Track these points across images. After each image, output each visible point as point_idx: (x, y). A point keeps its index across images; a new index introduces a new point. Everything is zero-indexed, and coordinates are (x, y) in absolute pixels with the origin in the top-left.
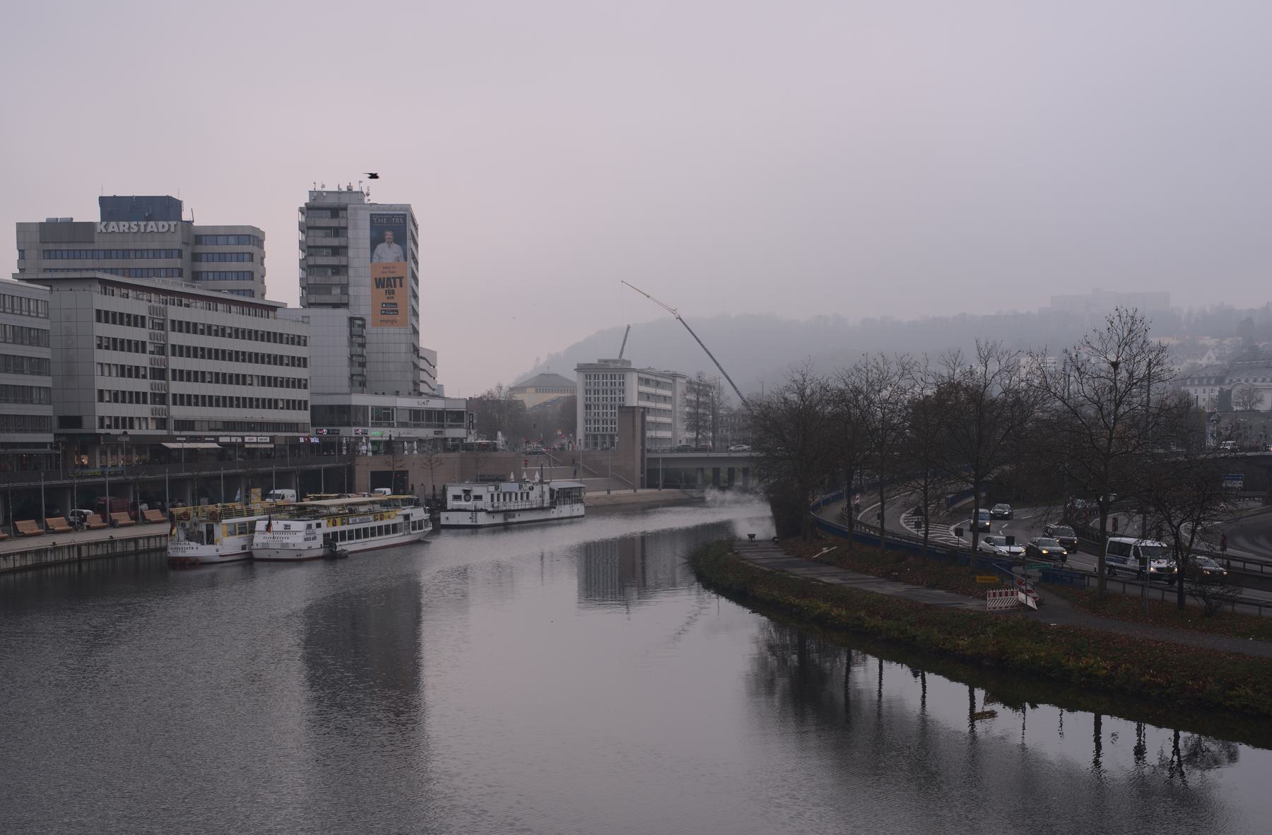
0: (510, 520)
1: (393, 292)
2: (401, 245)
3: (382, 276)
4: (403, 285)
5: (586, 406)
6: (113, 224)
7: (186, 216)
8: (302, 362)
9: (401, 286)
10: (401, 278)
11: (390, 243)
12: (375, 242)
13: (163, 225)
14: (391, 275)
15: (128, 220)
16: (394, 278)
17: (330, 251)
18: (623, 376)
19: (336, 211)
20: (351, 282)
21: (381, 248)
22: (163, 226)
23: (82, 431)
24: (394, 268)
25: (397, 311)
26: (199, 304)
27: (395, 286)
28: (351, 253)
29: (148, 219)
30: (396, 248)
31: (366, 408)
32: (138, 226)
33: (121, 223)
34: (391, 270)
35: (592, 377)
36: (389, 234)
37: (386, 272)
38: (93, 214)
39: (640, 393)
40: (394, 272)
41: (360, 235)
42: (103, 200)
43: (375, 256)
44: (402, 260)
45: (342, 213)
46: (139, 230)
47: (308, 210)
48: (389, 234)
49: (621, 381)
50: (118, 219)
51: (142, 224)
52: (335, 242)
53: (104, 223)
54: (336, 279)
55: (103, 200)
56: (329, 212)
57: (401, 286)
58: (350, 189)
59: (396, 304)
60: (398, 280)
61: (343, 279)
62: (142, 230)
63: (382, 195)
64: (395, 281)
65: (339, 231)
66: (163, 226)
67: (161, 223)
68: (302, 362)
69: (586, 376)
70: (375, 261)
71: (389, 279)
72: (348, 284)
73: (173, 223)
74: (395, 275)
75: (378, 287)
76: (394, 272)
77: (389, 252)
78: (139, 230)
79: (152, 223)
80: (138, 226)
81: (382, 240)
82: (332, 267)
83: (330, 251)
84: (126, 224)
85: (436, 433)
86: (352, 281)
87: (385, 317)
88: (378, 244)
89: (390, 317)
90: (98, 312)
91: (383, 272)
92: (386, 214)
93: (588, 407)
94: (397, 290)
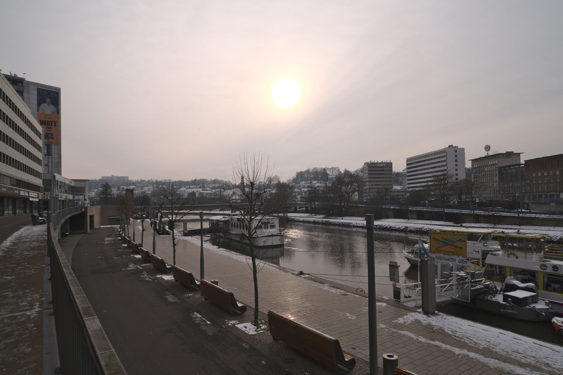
1: (51, 128)
2: (55, 106)
3: (44, 119)
4: (57, 125)
9: (55, 126)
10: (55, 122)
11: (49, 104)
16: (52, 122)
21: (43, 106)
24: (51, 116)
25: (53, 138)
27: (52, 125)
34: (50, 117)
36: (48, 100)
37: (46, 118)
40: (51, 119)
43: (40, 109)
44: (56, 113)
57: (55, 126)
59: (52, 134)
60: (53, 123)
64: (52, 124)
70: (40, 111)
71: (48, 121)
74: (51, 120)
76: (51, 119)
81: (45, 102)
88: (42, 103)
91: (45, 118)
92: (47, 90)
94: (53, 127)
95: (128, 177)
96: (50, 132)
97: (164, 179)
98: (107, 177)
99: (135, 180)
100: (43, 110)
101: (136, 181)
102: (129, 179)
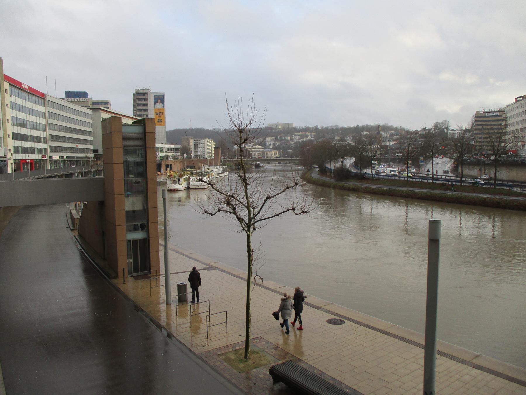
0: (218, 176)
1: (161, 116)
3: (157, 112)
6: (70, 99)
7: (89, 97)
9: (163, 115)
10: (163, 113)
11: (159, 103)
12: (155, 103)
13: (84, 100)
14: (160, 112)
15: (74, 98)
19: (144, 94)
21: (157, 104)
22: (84, 100)
23: (98, 153)
28: (149, 105)
29: (80, 98)
30: (161, 104)
31: (158, 147)
32: (77, 99)
33: (72, 99)
36: (159, 101)
38: (64, 96)
39: (208, 145)
41: (151, 101)
42: (66, 93)
43: (155, 106)
44: (163, 108)
45: (146, 95)
46: (77, 101)
48: (159, 101)
50: (71, 98)
51: (78, 99)
52: (144, 103)
53: (67, 99)
54: (145, 113)
55: (66, 93)
57: (163, 115)
58: (146, 89)
62: (78, 101)
63: (155, 89)
65: (146, 100)
66: (84, 100)
67: (84, 99)
70: (156, 108)
71: (159, 113)
73: (87, 99)
74: (161, 112)
75: (156, 115)
77: (159, 106)
78: (77, 101)
79: (81, 99)
80: (77, 99)
81: (157, 102)
82: (144, 109)
84: (74, 99)
85: (173, 154)
86: (149, 113)
87: (159, 123)
89: (160, 123)
93: (195, 148)
94: (162, 116)
96: (160, 119)
97: (330, 125)
99: (299, 127)
100: (157, 107)
101: (300, 128)
102: (294, 126)
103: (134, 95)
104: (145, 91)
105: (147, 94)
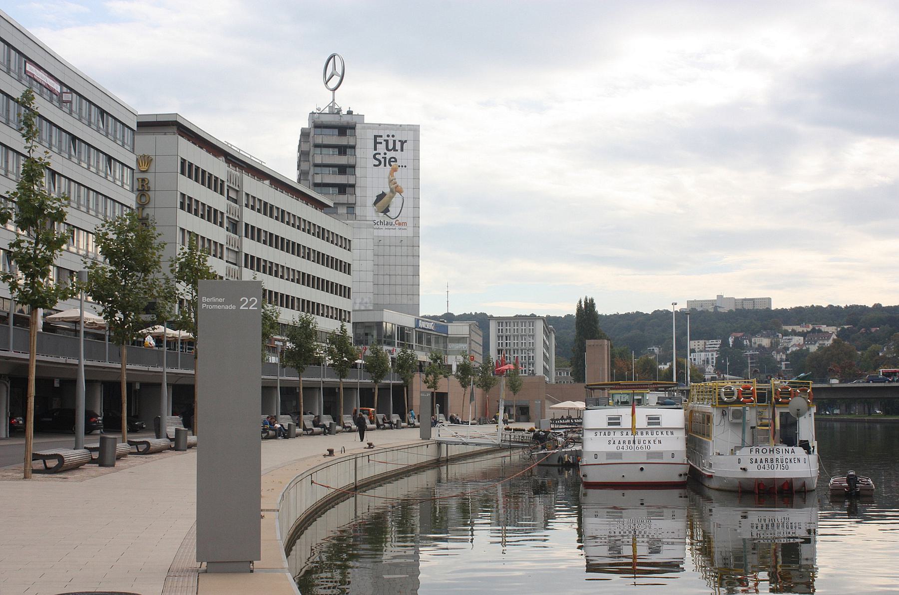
5: (499, 351)
8: (345, 268)
17: (336, 169)
18: (533, 322)
20: (358, 203)
26: (267, 182)
28: (358, 171)
35: (504, 324)
41: (364, 154)
47: (319, 126)
49: (531, 328)
52: (343, 160)
54: (343, 199)
56: (337, 130)
61: (351, 199)
68: (345, 268)
69: (499, 323)
72: (355, 204)
83: (336, 169)
90: (183, 161)
95: (770, 299)
98: (702, 303)
103: (305, 134)
104: (346, 120)
105: (353, 128)
